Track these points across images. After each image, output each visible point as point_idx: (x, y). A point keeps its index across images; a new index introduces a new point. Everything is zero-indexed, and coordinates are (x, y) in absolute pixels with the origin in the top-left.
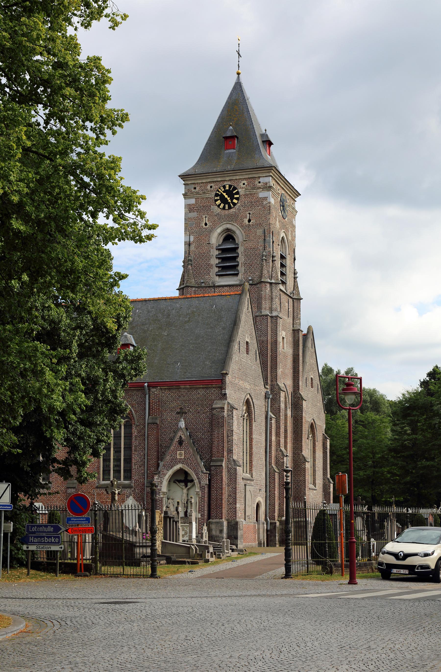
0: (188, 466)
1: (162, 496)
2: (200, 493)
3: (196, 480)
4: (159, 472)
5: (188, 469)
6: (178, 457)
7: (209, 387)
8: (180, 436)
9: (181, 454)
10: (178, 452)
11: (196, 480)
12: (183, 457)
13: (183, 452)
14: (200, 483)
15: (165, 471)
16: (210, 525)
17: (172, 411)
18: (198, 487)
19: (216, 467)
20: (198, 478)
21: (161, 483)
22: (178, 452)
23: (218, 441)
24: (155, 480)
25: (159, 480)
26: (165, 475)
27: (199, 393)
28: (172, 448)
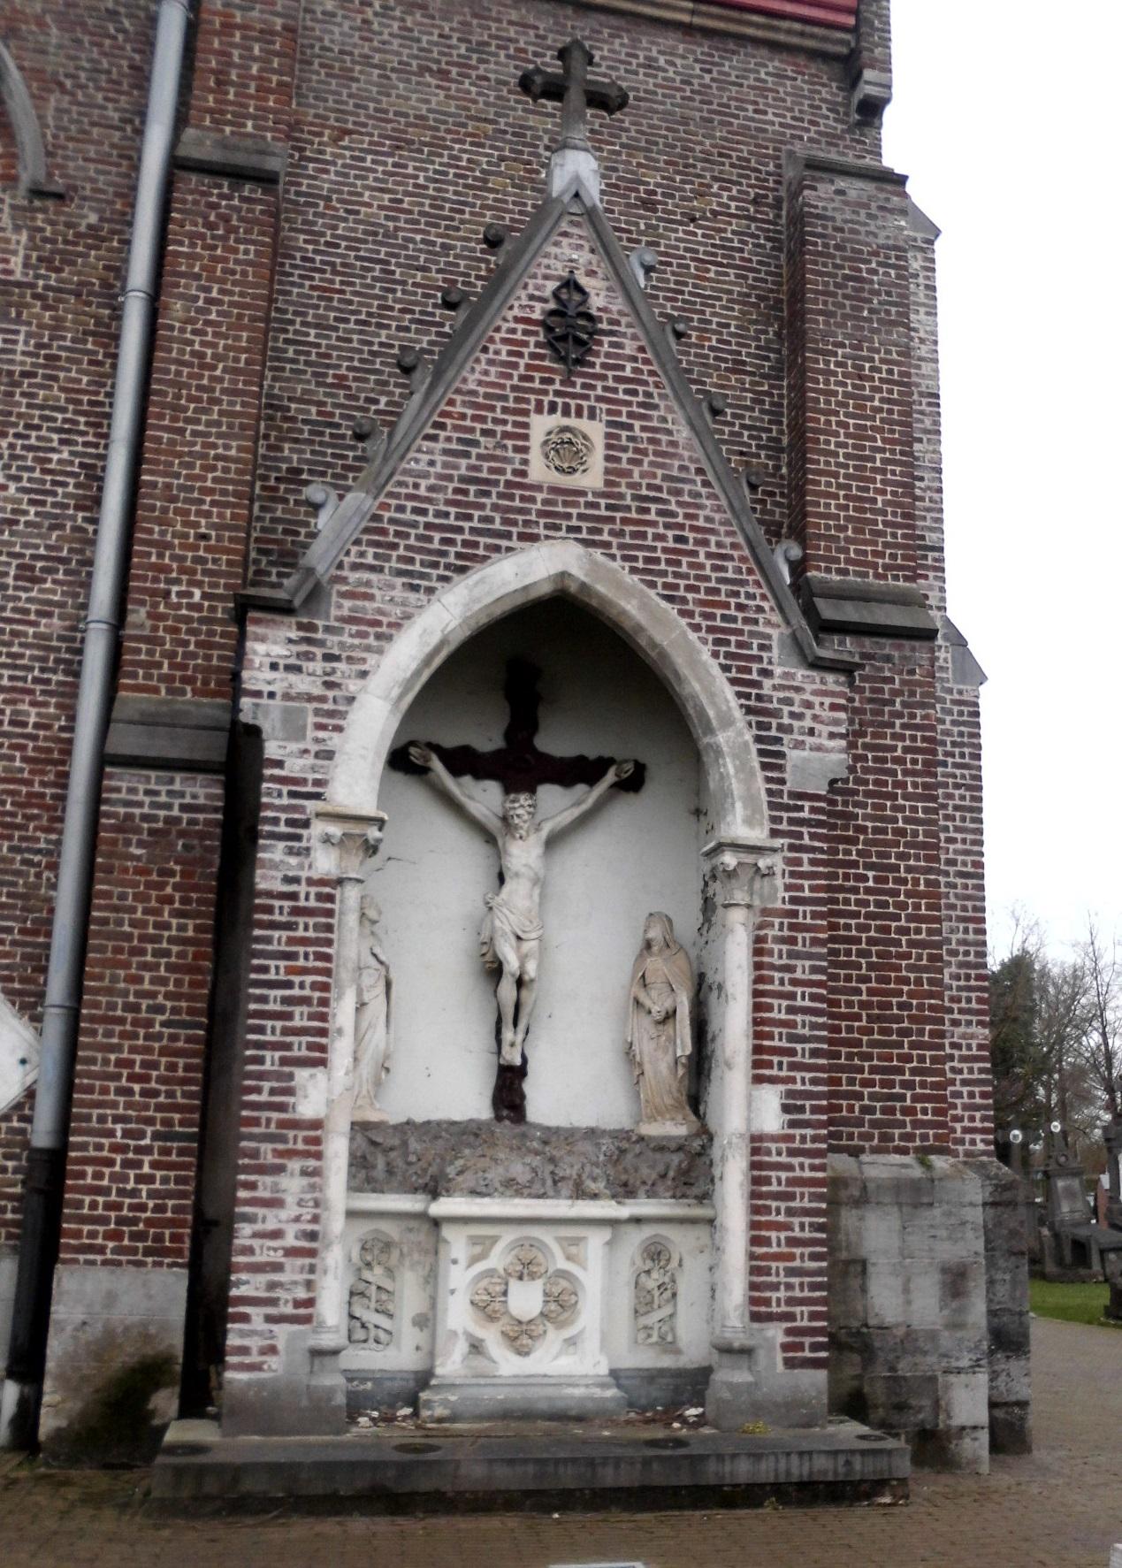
0: (648, 572)
1: (325, 863)
2: (777, 862)
3: (727, 722)
4: (316, 596)
5: (645, 605)
6: (539, 470)
7: (741, 39)
8: (570, 284)
9: (566, 449)
10: (541, 425)
11: (727, 722)
12: (592, 478)
13: (595, 430)
14: (772, 760)
15: (387, 593)
16: (848, 1218)
17: (401, 143)
18: (750, 800)
19: (868, 644)
20: (758, 711)
21: (333, 719)
22: (541, 425)
23: (860, 434)
24: (256, 676)
25: (302, 684)
26: (383, 631)
27: (650, 64)
28: (475, 375)
